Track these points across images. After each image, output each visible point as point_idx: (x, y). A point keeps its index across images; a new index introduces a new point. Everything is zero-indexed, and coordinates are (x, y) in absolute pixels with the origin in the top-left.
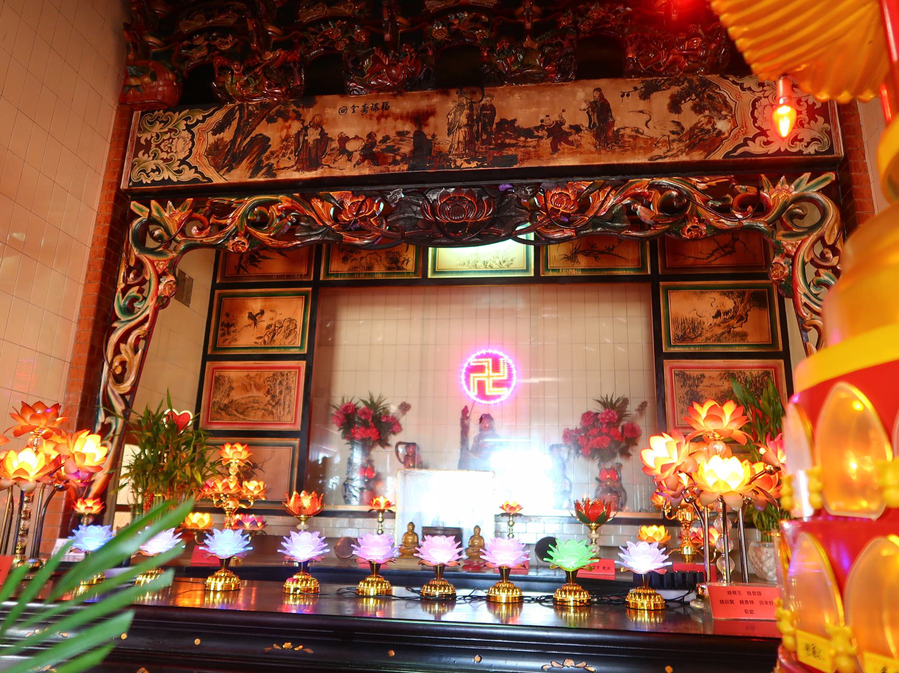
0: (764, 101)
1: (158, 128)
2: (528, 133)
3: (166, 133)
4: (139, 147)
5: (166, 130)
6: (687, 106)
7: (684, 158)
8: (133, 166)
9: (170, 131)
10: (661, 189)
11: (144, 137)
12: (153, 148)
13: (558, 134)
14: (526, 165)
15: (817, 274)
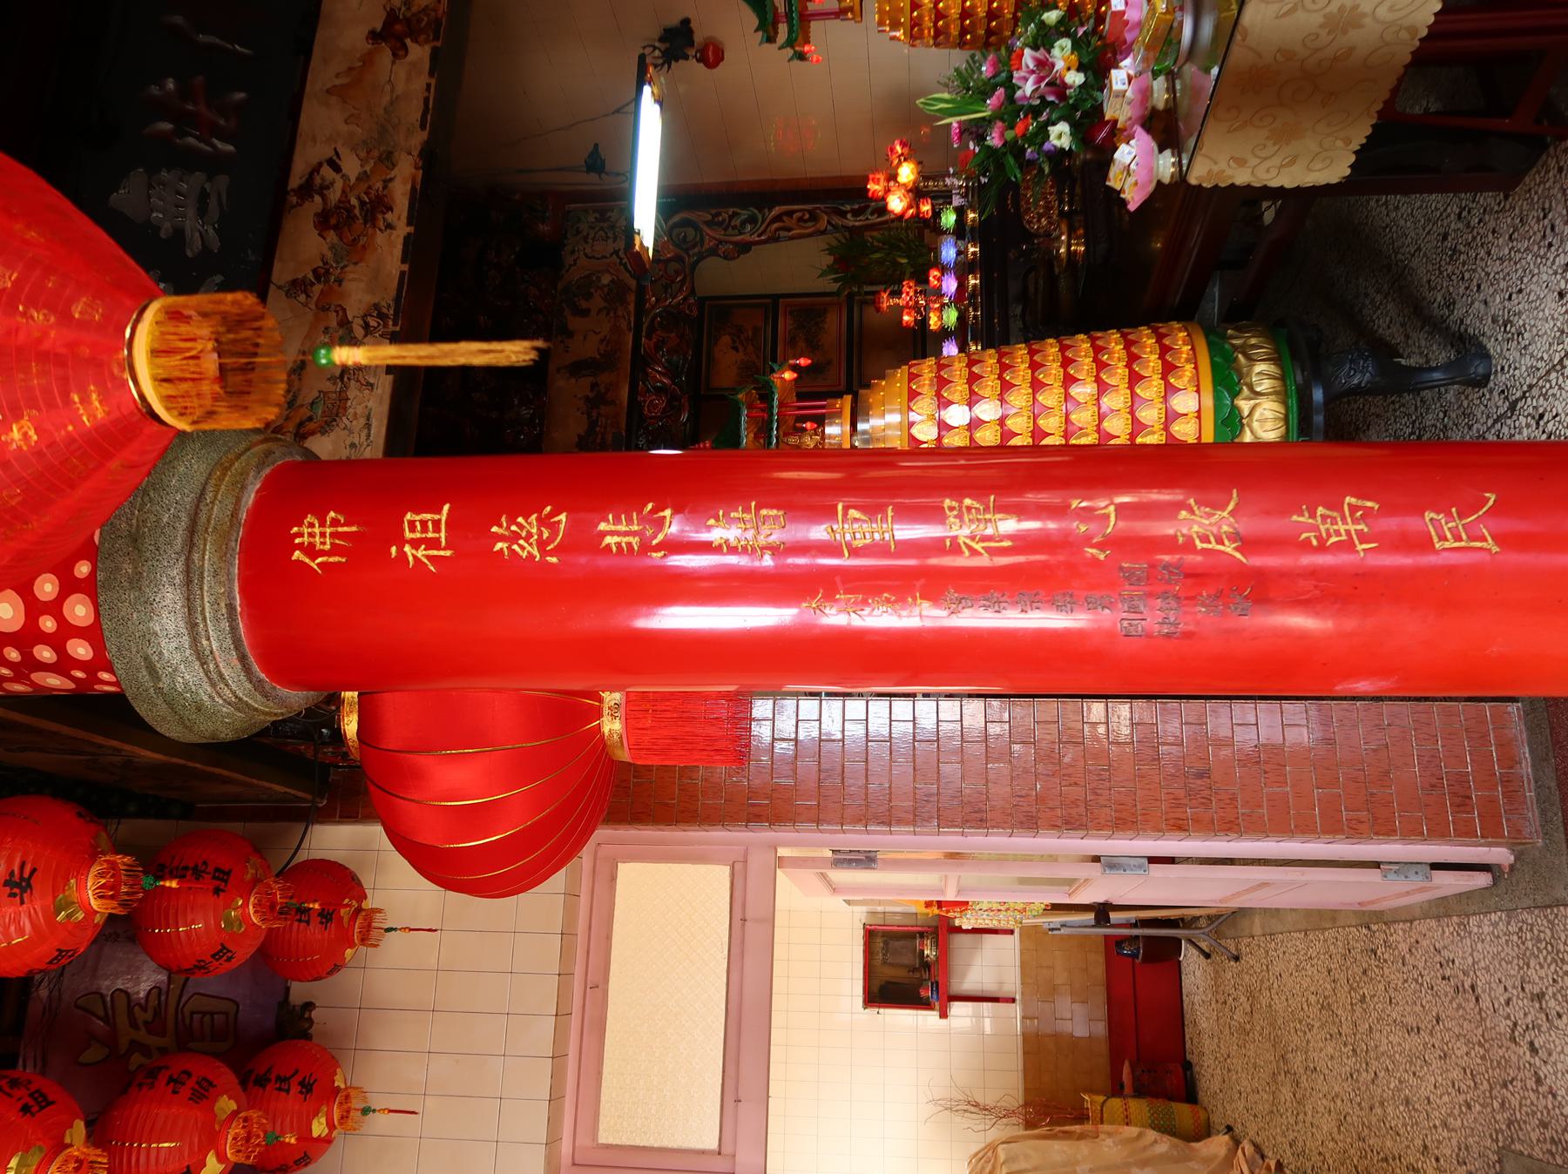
0: (588, 251)
2: (593, 424)
6: (584, 304)
7: (632, 307)
10: (652, 330)
13: (598, 400)
14: (623, 425)
15: (734, 228)
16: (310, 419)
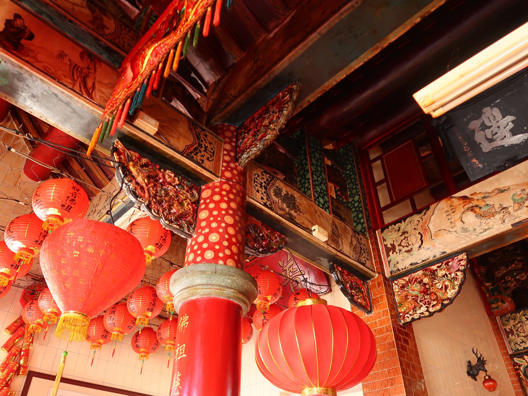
1: (512, 322)
3: (518, 324)
4: (507, 333)
5: (517, 322)
8: (510, 342)
9: (519, 322)
11: (508, 328)
12: (515, 332)
16: (480, 208)
